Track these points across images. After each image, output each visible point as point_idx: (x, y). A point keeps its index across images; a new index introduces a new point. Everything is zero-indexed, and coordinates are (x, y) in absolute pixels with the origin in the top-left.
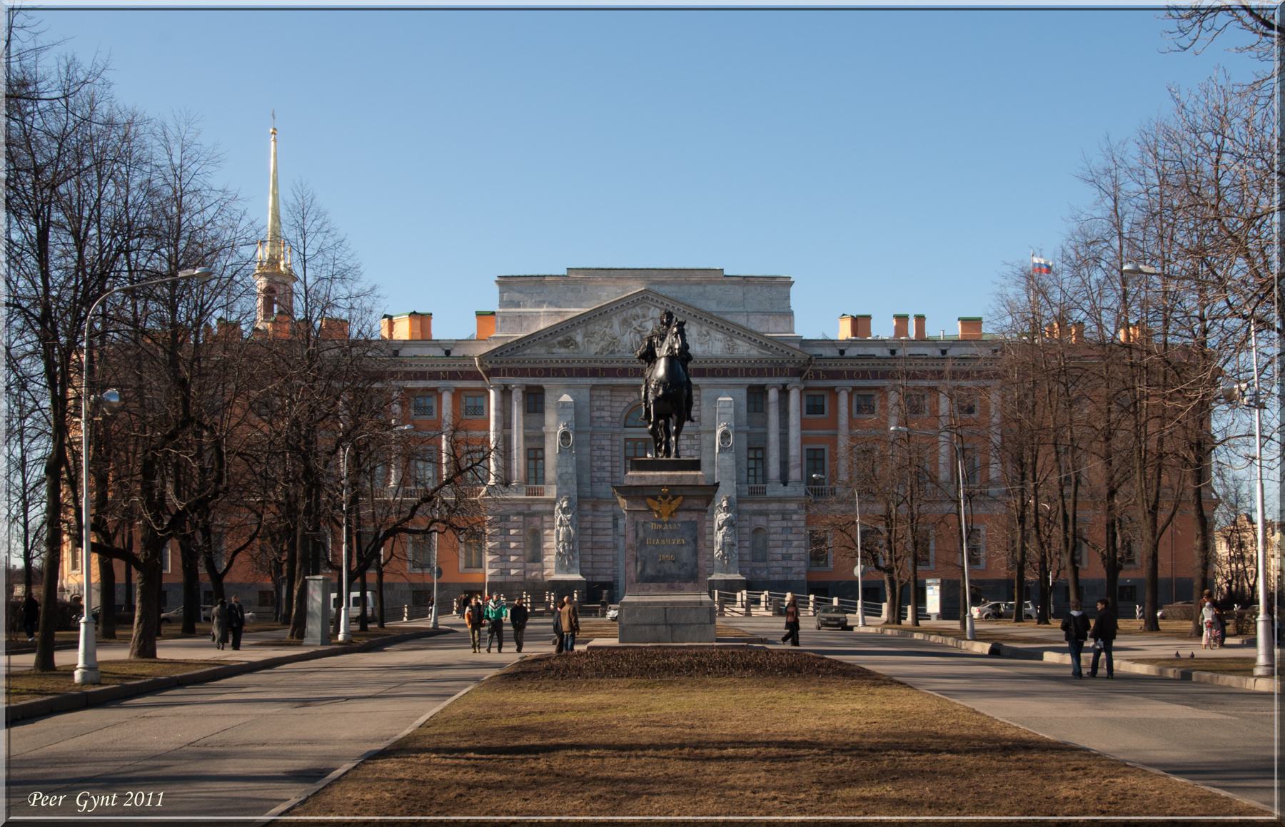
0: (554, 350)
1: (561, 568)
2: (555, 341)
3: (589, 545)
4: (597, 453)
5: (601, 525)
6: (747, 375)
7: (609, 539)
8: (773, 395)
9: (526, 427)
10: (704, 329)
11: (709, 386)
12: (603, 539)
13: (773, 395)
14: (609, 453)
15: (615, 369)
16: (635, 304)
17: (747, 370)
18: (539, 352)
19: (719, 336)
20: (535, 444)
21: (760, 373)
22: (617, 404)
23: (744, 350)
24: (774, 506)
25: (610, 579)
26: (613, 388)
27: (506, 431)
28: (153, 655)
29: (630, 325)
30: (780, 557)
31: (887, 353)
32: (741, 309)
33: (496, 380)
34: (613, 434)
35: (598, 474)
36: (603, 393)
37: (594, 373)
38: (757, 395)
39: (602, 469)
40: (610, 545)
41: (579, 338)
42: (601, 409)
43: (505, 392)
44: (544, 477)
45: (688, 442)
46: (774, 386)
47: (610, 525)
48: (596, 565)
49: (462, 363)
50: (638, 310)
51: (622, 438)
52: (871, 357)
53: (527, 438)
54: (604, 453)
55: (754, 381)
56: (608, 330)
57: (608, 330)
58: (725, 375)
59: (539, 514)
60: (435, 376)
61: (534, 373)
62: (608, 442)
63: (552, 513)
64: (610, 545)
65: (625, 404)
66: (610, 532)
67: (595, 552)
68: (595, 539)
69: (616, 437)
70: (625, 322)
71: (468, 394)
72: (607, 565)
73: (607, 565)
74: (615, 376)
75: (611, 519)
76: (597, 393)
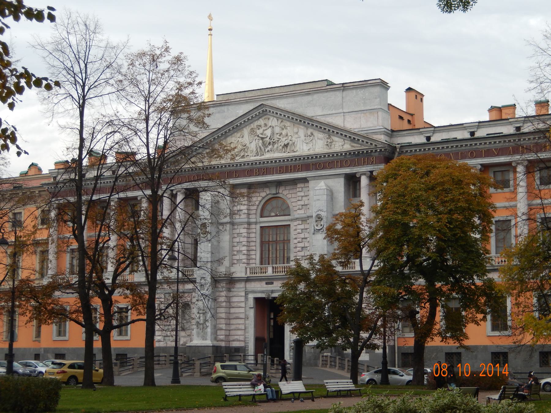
3: (223, 315)
4: (237, 240)
6: (342, 166)
8: (364, 181)
10: (310, 131)
11: (315, 178)
13: (364, 181)
14: (245, 239)
15: (244, 170)
16: (258, 117)
17: (341, 162)
19: (321, 135)
21: (352, 164)
23: (341, 146)
25: (242, 344)
26: (250, 186)
31: (468, 136)
32: (341, 111)
34: (249, 224)
35: (237, 257)
38: (352, 182)
39: (239, 251)
40: (242, 316)
43: (173, 197)
45: (302, 227)
46: (364, 174)
47: (243, 299)
48: (232, 333)
50: (261, 122)
51: (258, 227)
52: (455, 140)
54: (242, 239)
55: (348, 170)
57: (240, 139)
58: (324, 168)
62: (245, 230)
65: (260, 199)
66: (243, 305)
67: (233, 322)
68: (232, 310)
69: (253, 226)
70: (252, 131)
73: (240, 332)
74: (245, 176)
75: (243, 294)
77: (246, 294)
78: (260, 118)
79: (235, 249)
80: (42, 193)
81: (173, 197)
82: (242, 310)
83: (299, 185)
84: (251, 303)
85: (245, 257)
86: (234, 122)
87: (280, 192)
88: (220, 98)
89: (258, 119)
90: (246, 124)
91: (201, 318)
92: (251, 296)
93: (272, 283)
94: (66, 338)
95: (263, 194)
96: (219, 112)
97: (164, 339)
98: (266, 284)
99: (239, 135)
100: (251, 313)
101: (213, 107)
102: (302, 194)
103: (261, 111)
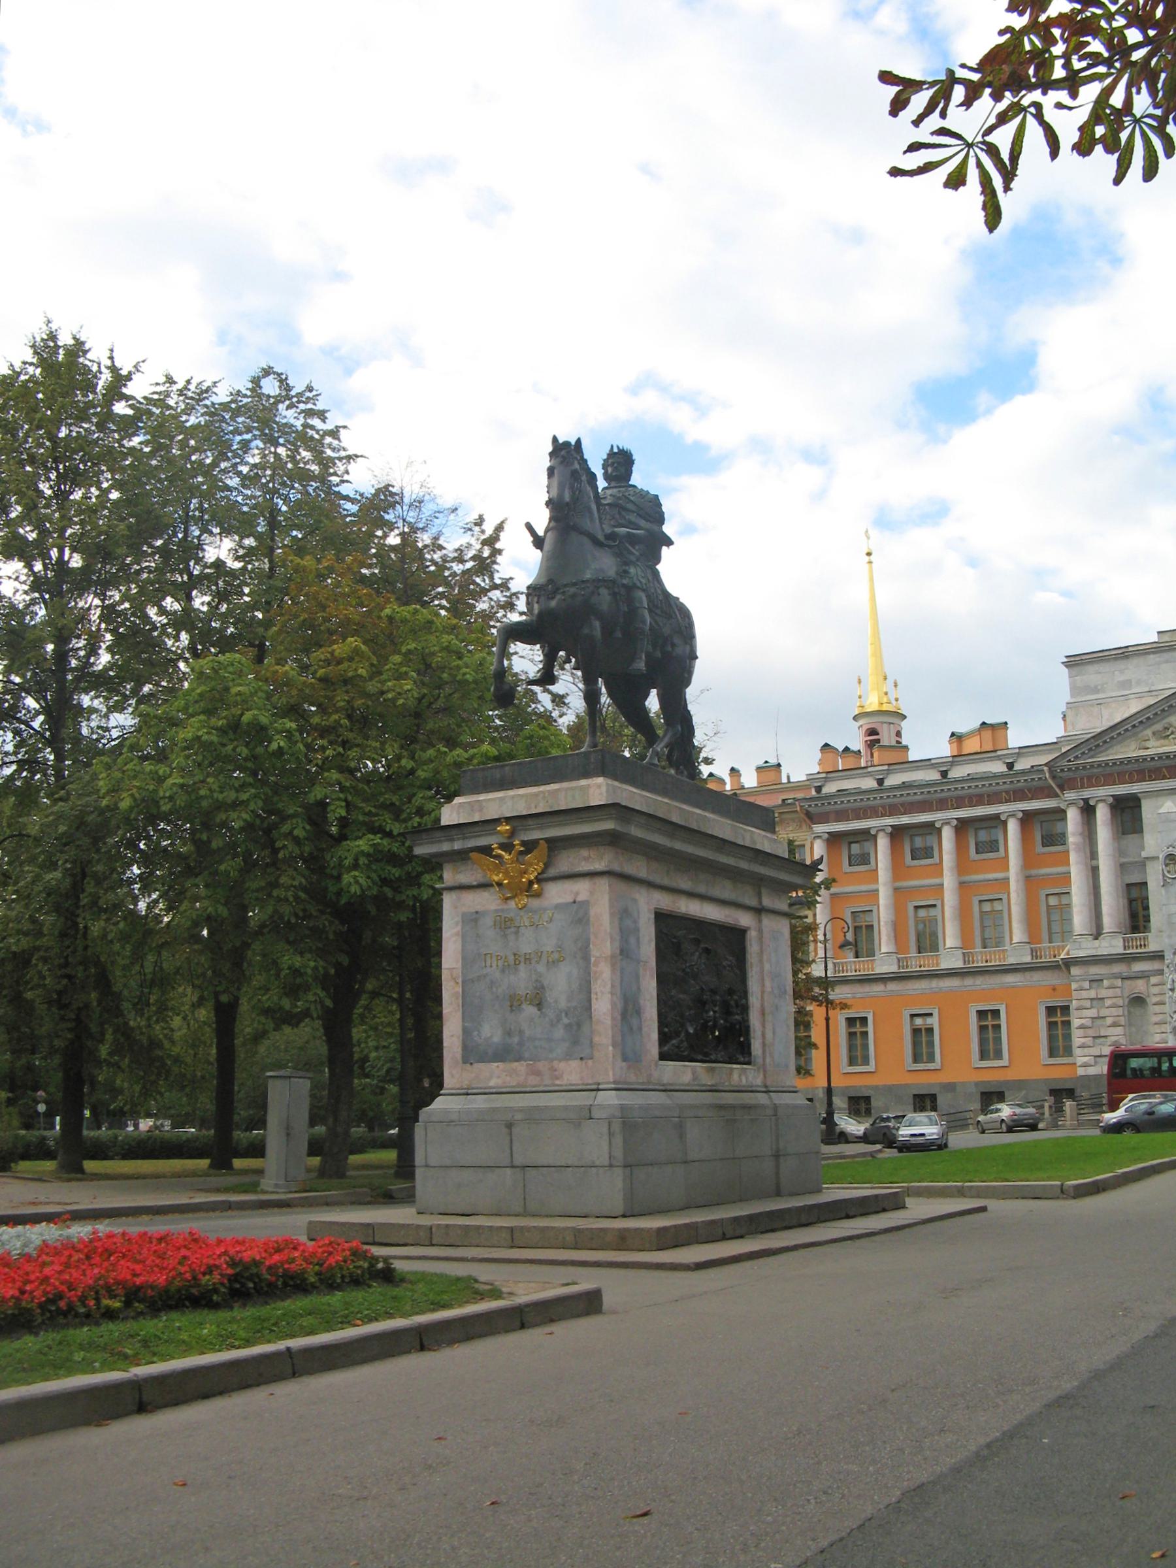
0: (1148, 744)
2: (1149, 732)
9: (1120, 852)
18: (1128, 750)
20: (1135, 878)
27: (1094, 863)
28: (230, 1167)
33: (1070, 795)
43: (1088, 810)
44: (1147, 919)
49: (1028, 778)
53: (1122, 868)
60: (994, 798)
61: (1121, 778)
63: (1160, 972)
71: (1043, 818)
80: (784, 816)
81: (1088, 810)
88: (1166, 638)
94: (871, 1067)
96: (1167, 662)
97: (1096, 1063)
101: (1154, 653)
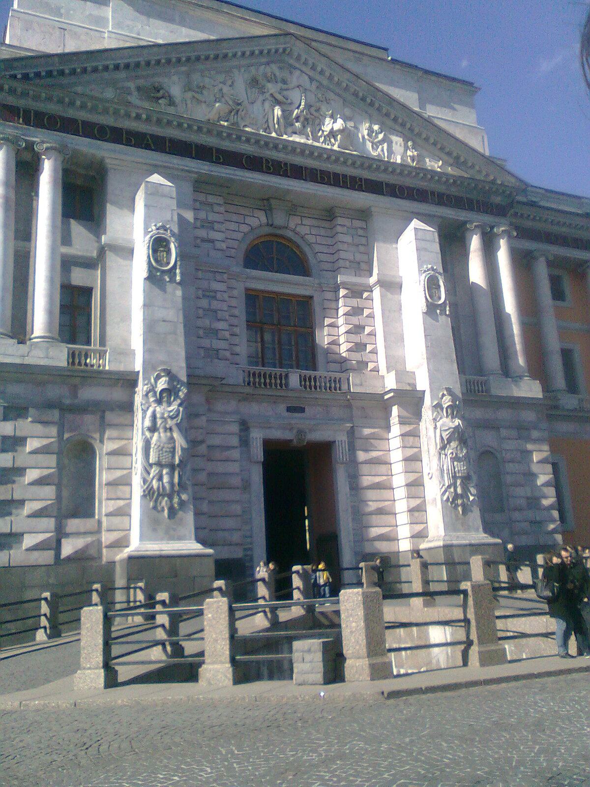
1: (151, 525)
5: (216, 440)
7: (234, 467)
12: (221, 468)
22: (233, 226)
24: (504, 414)
29: (262, 90)
30: (523, 502)
36: (211, 199)
37: (203, 153)
40: (236, 481)
41: (176, 91)
42: (209, 225)
47: (235, 441)
54: (215, 305)
56: (226, 89)
59: (100, 409)
64: (236, 481)
65: (245, 228)
66: (236, 454)
70: (254, 83)
72: (230, 523)
73: (230, 523)
75: (235, 428)
76: (202, 197)
77: (245, 427)
78: (272, 62)
79: (200, 323)
82: (234, 467)
83: (340, 221)
84: (258, 452)
85: (222, 345)
86: (225, 44)
87: (292, 225)
89: (268, 64)
90: (244, 62)
91: (166, 479)
92: (257, 436)
93: (302, 410)
95: (254, 222)
98: (289, 409)
99: (221, 77)
100: (257, 476)
102: (348, 239)
103: (281, 47)
